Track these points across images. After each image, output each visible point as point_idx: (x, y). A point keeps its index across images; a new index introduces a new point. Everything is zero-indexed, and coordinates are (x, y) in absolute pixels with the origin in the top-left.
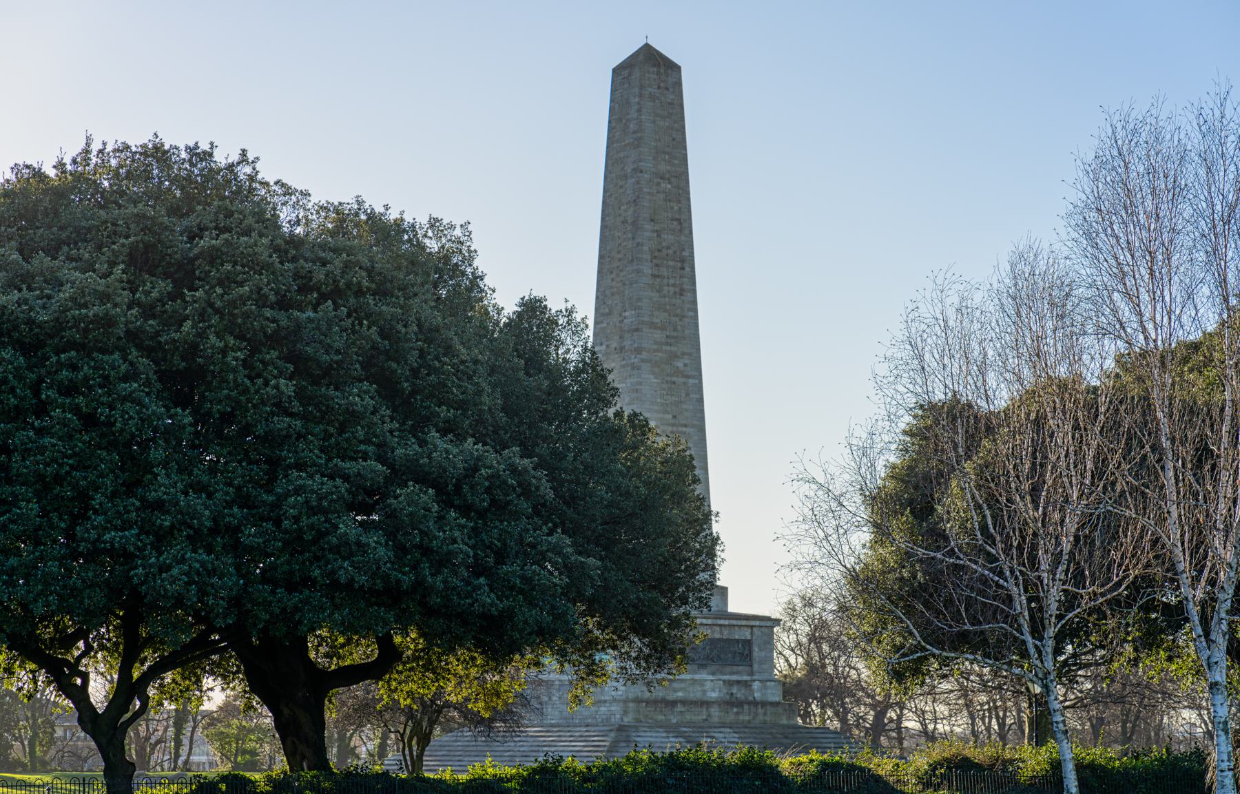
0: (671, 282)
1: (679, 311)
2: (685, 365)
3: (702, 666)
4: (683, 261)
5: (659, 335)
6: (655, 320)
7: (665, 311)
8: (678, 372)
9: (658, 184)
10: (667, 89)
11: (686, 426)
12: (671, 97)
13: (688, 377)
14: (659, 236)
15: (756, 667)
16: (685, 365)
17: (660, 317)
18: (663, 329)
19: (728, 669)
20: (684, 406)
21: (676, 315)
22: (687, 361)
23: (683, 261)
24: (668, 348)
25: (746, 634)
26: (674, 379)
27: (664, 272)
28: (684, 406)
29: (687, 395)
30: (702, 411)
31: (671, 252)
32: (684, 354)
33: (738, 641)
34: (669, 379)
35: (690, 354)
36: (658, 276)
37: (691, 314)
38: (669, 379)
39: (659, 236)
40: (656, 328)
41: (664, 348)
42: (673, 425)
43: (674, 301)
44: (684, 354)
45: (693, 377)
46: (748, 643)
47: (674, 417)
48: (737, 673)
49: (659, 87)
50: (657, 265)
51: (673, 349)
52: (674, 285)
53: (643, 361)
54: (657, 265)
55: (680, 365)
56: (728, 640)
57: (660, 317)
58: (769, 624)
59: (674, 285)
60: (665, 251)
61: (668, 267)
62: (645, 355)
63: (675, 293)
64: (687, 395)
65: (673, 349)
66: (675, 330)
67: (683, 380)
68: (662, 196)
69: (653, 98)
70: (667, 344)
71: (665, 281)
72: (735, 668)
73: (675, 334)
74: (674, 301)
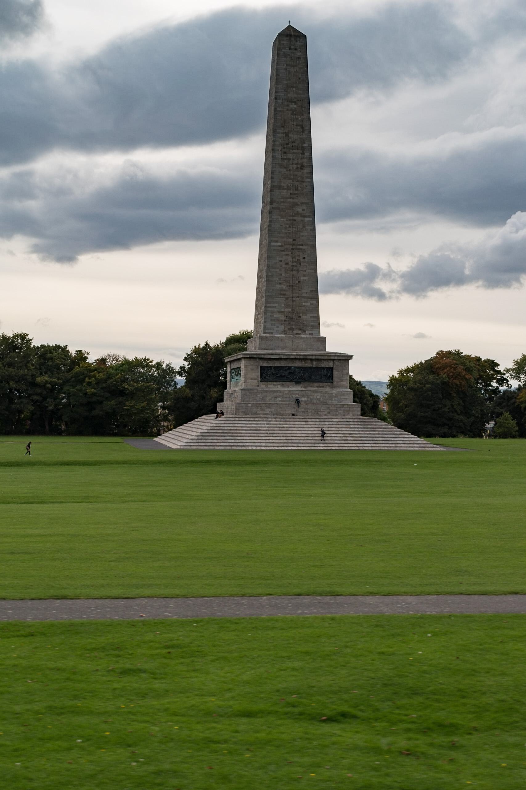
0: (295, 162)
1: (300, 179)
2: (303, 210)
3: (298, 383)
4: (303, 149)
5: (285, 193)
6: (282, 185)
7: (290, 179)
8: (298, 214)
9: (288, 105)
10: (296, 49)
11: (302, 245)
12: (299, 54)
13: (305, 217)
14: (287, 135)
15: (335, 383)
16: (303, 210)
17: (286, 183)
18: (288, 189)
19: (316, 384)
20: (302, 234)
21: (298, 181)
22: (305, 208)
23: (303, 149)
24: (291, 200)
25: (331, 364)
26: (295, 218)
27: (290, 156)
28: (302, 234)
29: (304, 227)
30: (315, 236)
31: (295, 144)
32: (302, 203)
33: (324, 368)
34: (291, 218)
35: (307, 204)
36: (286, 159)
37: (309, 180)
38: (291, 218)
39: (287, 135)
40: (283, 189)
41: (289, 200)
42: (294, 245)
43: (296, 173)
44: (302, 203)
45: (308, 217)
46: (332, 369)
47: (294, 240)
48: (323, 387)
49: (290, 49)
50: (285, 153)
51: (295, 201)
52: (296, 164)
53: (273, 208)
54: (285, 153)
55: (299, 209)
56: (317, 368)
57: (286, 183)
58: (346, 358)
59: (296, 164)
60: (290, 146)
61: (293, 153)
62: (275, 205)
63: (297, 168)
64: (304, 227)
65: (295, 201)
66: (297, 190)
67: (302, 218)
68: (290, 112)
69: (285, 55)
70: (290, 198)
71: (291, 162)
72: (321, 384)
73: (297, 192)
74: (296, 173)
